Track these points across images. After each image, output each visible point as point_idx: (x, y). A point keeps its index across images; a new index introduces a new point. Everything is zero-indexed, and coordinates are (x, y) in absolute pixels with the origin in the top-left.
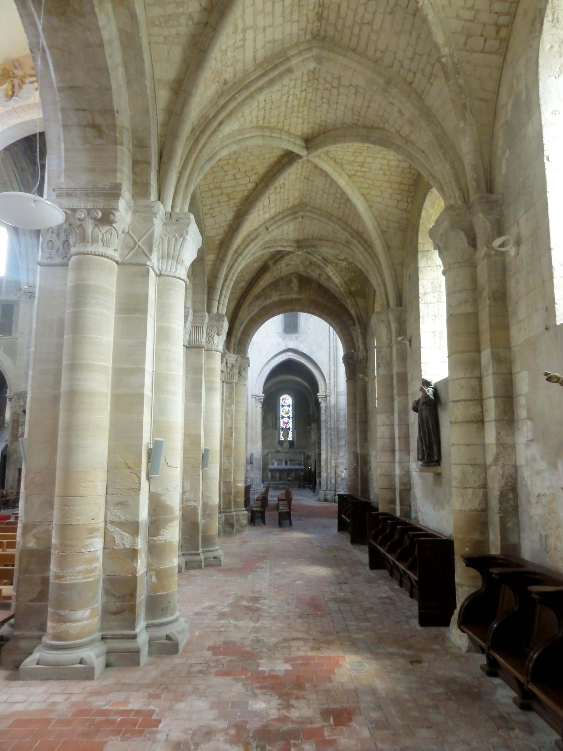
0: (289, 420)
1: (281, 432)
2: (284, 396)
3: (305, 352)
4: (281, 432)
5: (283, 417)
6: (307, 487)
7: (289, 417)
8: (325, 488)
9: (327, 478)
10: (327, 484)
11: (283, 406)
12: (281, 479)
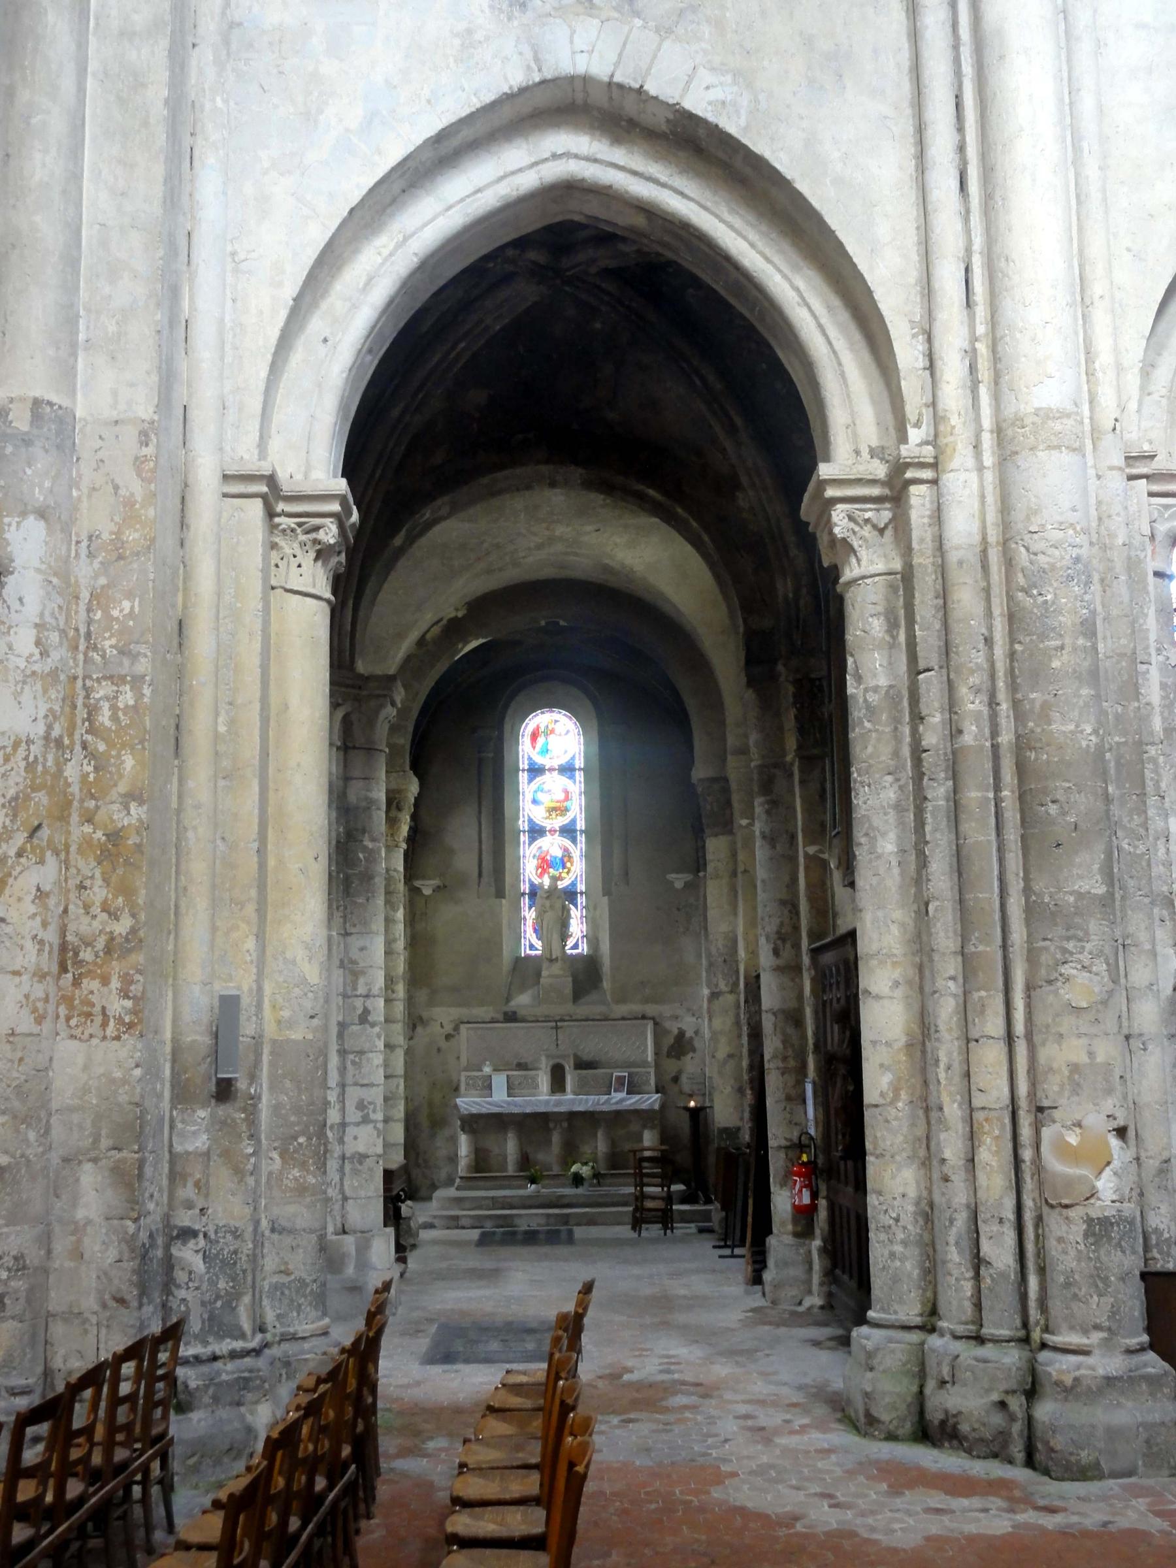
0: (567, 843)
1: (529, 915)
2: (540, 719)
3: (697, 103)
4: (529, 915)
5: (536, 832)
6: (686, 1218)
7: (568, 831)
8: (911, 1312)
9: (928, 1213)
10: (931, 1270)
11: (536, 771)
12: (529, 1170)
